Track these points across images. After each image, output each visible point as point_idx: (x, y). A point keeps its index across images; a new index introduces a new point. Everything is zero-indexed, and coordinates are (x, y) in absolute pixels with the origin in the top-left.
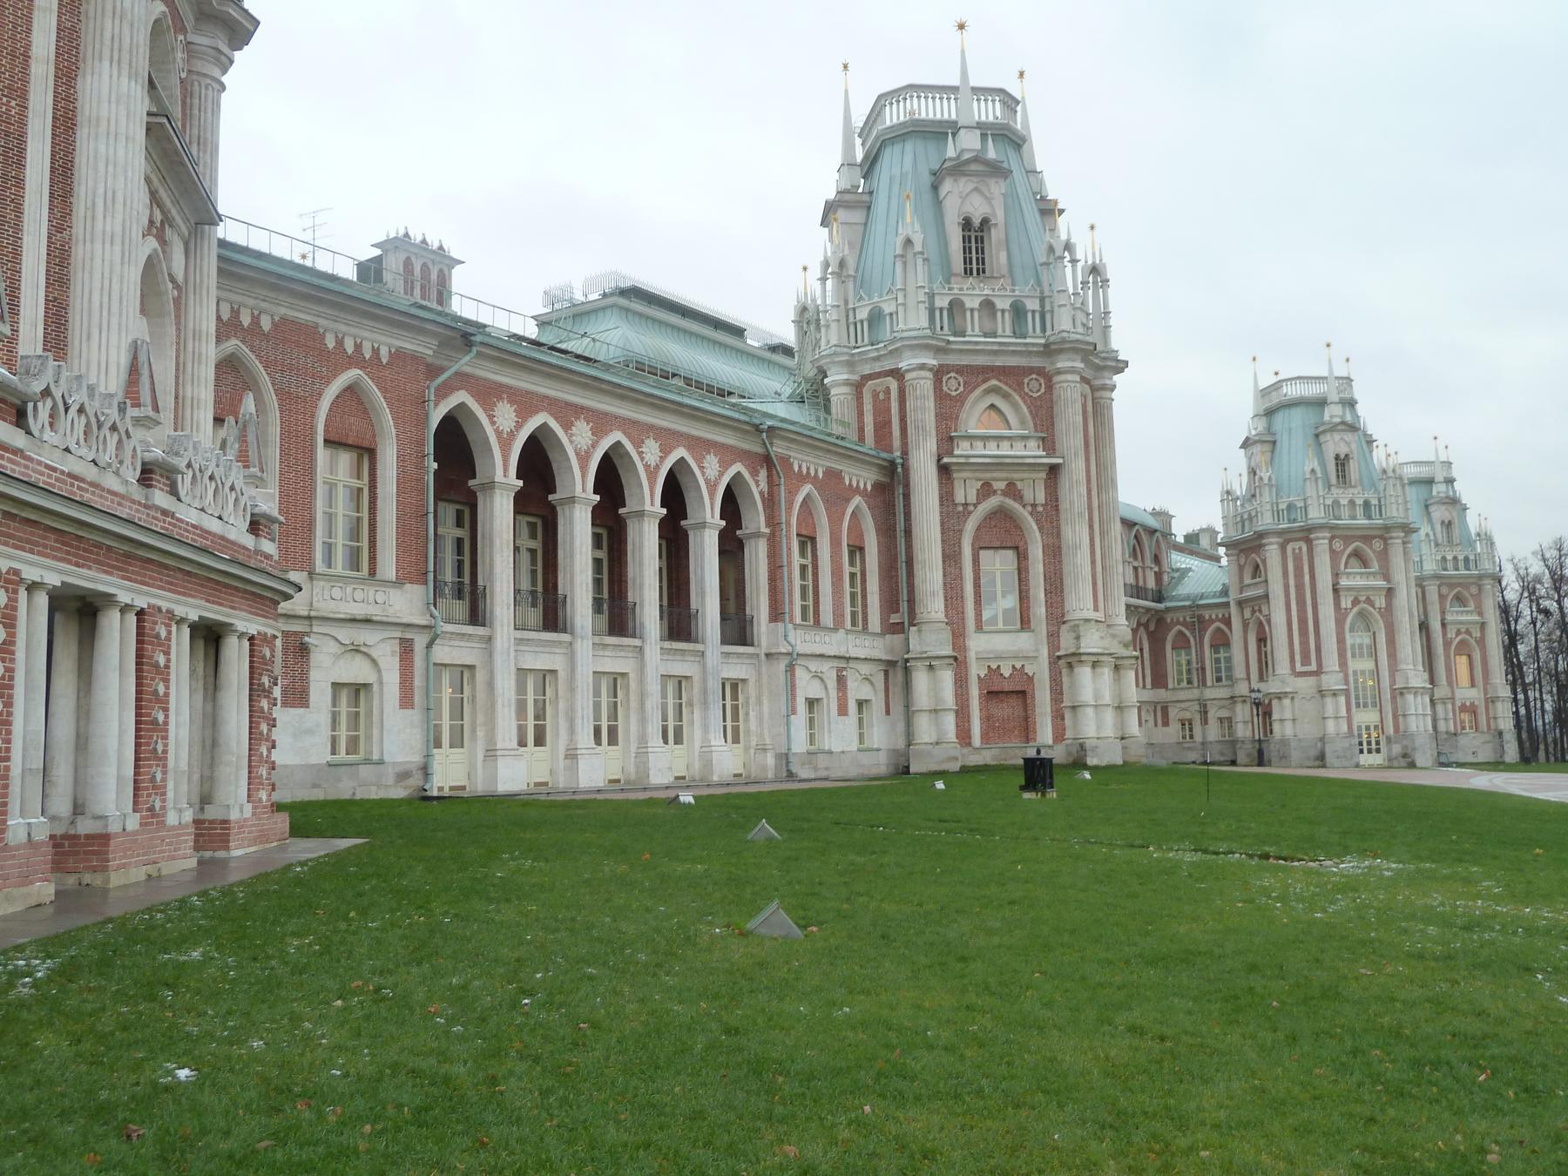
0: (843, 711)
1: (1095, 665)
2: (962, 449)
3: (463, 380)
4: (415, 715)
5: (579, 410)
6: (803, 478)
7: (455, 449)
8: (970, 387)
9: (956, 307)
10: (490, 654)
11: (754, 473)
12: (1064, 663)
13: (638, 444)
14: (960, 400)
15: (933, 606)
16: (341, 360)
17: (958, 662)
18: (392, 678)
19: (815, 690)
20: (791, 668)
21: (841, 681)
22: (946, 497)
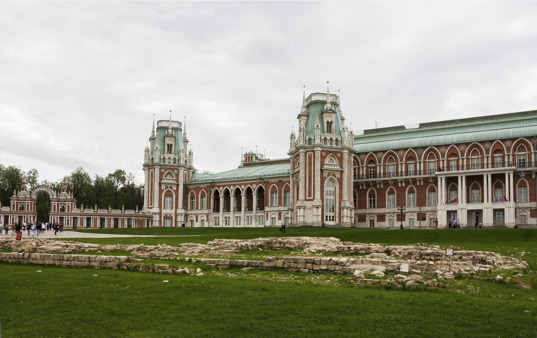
0: (280, 219)
1: (300, 208)
3: (217, 186)
6: (272, 183)
7: (217, 193)
11: (263, 185)
13: (241, 187)
19: (273, 216)
20: (267, 214)
21: (280, 215)
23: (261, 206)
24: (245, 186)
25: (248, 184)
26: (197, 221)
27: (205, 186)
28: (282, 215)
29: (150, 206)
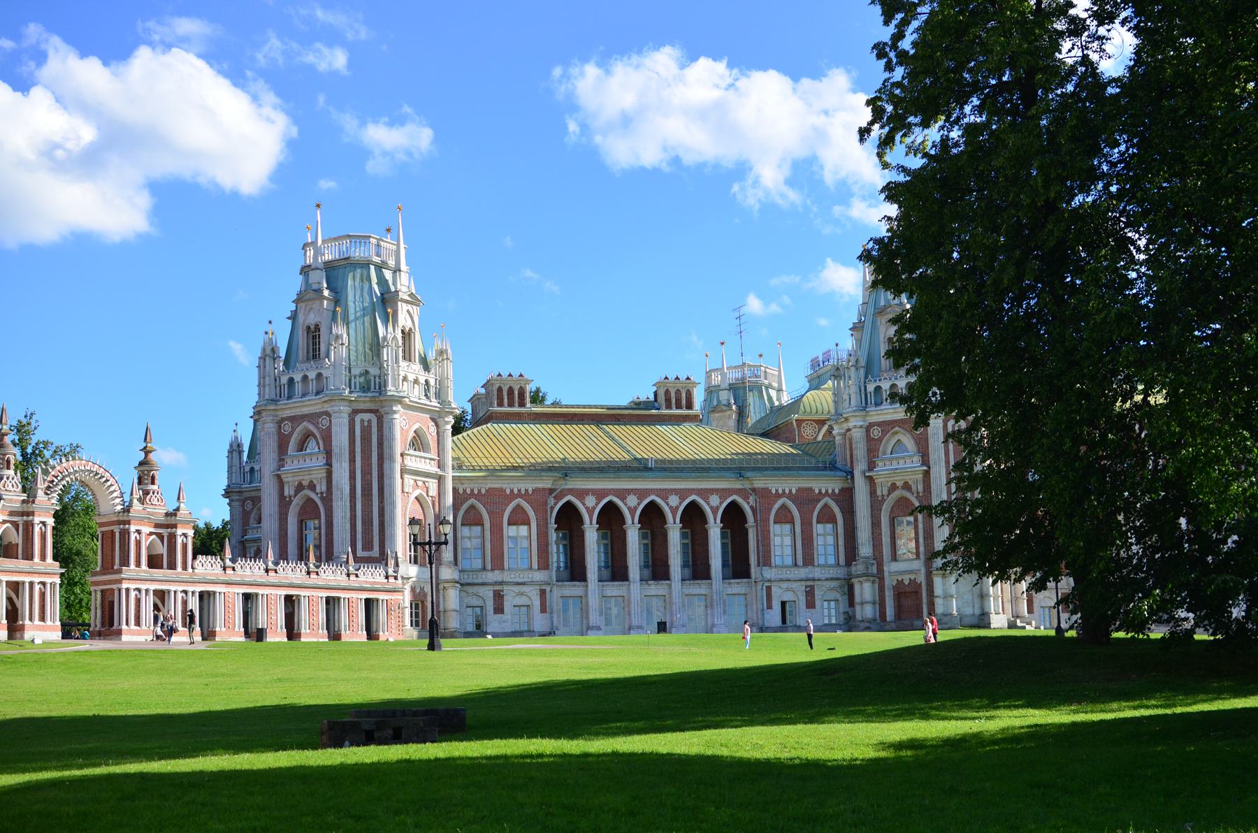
0: (811, 604)
2: (881, 467)
3: (571, 491)
4: (547, 615)
5: (629, 491)
6: (778, 496)
7: (569, 518)
8: (884, 433)
9: (878, 389)
10: (586, 591)
11: (746, 498)
12: (929, 576)
13: (665, 499)
14: (880, 440)
15: (865, 550)
16: (513, 496)
17: (880, 576)
18: (537, 603)
19: (787, 597)
20: (769, 589)
21: (810, 593)
22: (873, 493)
23: (738, 567)
24: (682, 499)
25: (691, 491)
26: (499, 609)
27: (529, 486)
28: (818, 594)
29: (360, 553)
